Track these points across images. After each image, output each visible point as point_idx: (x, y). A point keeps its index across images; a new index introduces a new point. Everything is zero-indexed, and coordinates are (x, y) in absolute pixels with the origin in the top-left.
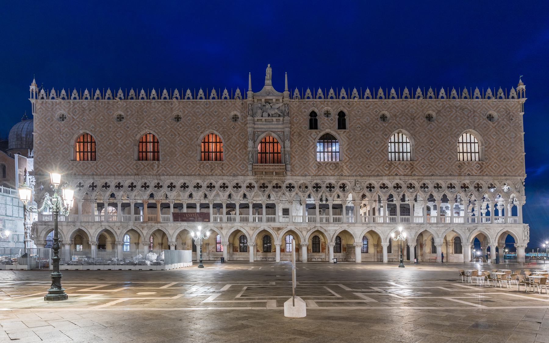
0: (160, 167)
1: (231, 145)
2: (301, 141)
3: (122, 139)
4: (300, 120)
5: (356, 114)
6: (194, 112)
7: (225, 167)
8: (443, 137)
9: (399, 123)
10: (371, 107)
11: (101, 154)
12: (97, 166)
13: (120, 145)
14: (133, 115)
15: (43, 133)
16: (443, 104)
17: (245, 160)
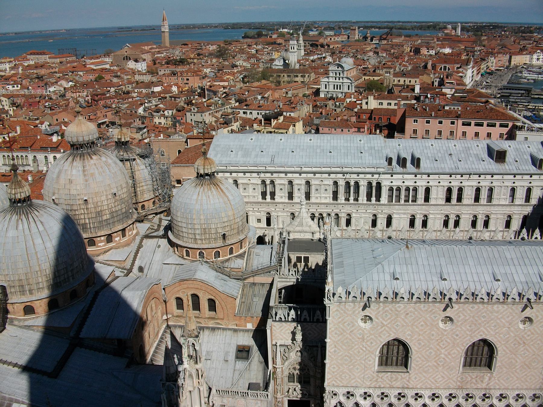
0: (493, 379)
11: (417, 365)
12: (410, 378)
13: (443, 356)
14: (466, 320)
15: (338, 341)
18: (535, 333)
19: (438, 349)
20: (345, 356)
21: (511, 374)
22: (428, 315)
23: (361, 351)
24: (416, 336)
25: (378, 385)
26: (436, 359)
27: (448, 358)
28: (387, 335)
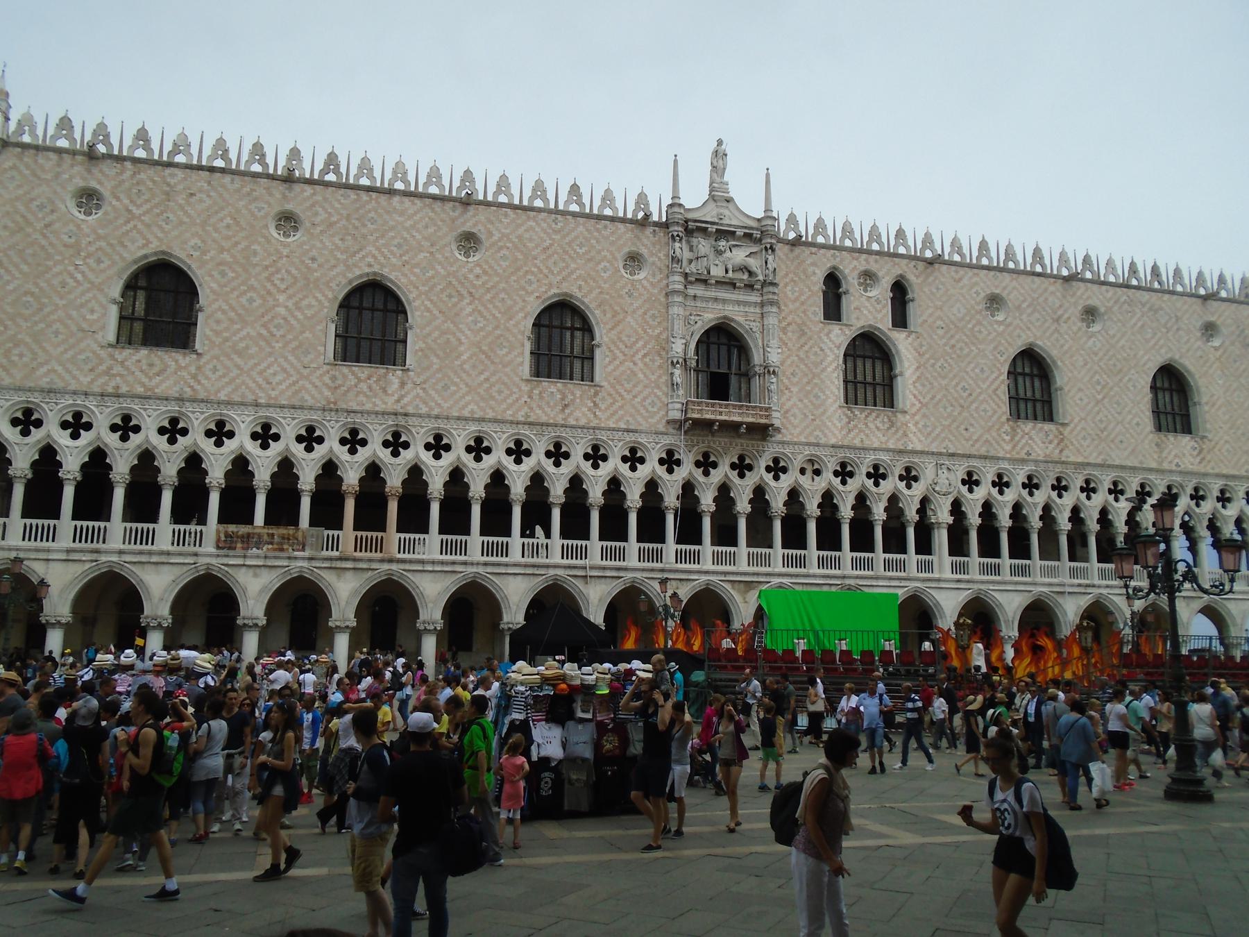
0: (410, 386)
1: (620, 338)
2: (806, 348)
3: (290, 291)
4: (802, 293)
5: (932, 293)
6: (520, 237)
7: (603, 399)
8: (1121, 370)
9: (1029, 329)
10: (965, 281)
11: (217, 333)
12: (199, 368)
13: (282, 311)
14: (331, 225)
16: (1115, 293)
17: (658, 387)
18: (490, 271)
19: (269, 293)
20: (26, 293)
21: (452, 375)
22: (241, 203)
23: (70, 281)
24: (213, 252)
25: (113, 384)
26: (266, 318)
27: (295, 317)
28: (141, 242)
